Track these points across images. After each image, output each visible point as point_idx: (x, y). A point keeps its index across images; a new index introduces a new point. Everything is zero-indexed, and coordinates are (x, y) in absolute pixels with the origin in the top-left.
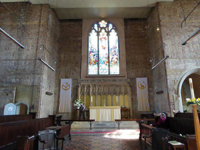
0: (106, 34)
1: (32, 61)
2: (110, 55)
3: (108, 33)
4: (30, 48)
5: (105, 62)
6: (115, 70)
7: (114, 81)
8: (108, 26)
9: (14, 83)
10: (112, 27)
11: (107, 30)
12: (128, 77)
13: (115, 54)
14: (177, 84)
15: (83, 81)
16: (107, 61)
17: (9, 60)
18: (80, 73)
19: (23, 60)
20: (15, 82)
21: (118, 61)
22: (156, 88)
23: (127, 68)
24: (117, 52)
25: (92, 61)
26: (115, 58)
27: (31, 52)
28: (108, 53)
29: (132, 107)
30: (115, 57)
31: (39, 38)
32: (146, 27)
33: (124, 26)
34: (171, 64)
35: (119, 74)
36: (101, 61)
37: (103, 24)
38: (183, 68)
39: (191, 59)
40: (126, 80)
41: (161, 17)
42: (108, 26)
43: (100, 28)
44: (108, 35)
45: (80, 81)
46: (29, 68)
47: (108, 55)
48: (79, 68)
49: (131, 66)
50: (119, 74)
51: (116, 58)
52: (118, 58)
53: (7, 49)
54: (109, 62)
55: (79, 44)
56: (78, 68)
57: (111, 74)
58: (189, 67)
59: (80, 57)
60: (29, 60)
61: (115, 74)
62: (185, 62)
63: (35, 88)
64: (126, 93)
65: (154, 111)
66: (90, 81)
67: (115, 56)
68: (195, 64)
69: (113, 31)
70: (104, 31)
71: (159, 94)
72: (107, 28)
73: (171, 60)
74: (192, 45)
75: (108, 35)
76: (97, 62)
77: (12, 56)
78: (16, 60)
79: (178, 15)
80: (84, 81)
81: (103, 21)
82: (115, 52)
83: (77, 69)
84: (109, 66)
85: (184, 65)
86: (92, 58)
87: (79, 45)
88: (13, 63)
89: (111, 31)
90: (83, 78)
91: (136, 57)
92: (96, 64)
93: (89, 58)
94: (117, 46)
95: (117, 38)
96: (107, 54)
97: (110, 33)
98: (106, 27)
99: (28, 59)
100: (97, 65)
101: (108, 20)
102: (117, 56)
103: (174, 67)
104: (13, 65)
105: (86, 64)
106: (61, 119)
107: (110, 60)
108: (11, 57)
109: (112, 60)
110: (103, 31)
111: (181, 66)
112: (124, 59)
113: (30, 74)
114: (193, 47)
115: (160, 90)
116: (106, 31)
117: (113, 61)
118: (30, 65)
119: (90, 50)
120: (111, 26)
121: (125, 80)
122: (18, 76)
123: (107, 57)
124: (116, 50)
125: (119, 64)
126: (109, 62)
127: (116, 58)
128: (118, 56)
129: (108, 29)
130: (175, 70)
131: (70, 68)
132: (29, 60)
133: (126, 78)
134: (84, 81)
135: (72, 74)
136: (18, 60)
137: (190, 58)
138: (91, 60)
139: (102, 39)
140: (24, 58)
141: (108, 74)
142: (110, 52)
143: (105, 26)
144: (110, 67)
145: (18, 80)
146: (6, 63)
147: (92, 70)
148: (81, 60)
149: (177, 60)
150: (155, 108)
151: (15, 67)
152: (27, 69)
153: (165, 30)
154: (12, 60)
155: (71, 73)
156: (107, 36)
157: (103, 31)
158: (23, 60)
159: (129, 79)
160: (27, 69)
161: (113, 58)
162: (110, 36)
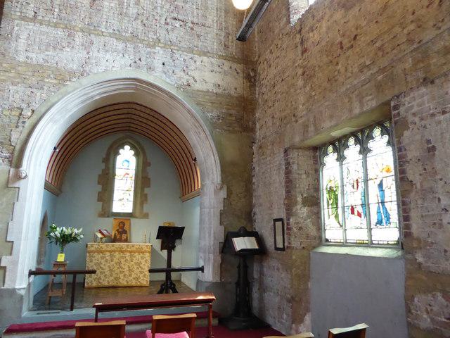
14: (28, 124)
34: (22, 41)
58: (101, 69)
62: (88, 46)
68: (128, 60)
103: (36, 57)
130: (38, 69)
137: (118, 35)
149: (60, 33)
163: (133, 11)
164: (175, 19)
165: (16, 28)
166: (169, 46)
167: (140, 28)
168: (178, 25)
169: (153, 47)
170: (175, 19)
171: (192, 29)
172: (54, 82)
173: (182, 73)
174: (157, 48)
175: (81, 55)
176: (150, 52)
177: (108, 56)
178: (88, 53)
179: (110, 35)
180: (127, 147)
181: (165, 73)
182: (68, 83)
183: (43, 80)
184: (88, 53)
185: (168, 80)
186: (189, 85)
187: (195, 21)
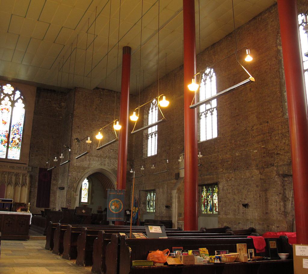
0: (10, 103)
2: (11, 133)
3: (13, 103)
5: (3, 142)
8: (14, 93)
10: (19, 96)
11: (12, 99)
13: (18, 133)
16: (6, 140)
21: (20, 143)
22: (60, 182)
23: (30, 153)
24: (21, 130)
26: (17, 138)
28: (8, 131)
30: (18, 136)
32: (63, 104)
33: (36, 97)
35: (18, 159)
37: (8, 89)
39: (97, 157)
41: (75, 105)
42: (14, 93)
43: (4, 94)
44: (13, 106)
47: (8, 132)
50: (18, 159)
51: (18, 139)
52: (21, 139)
54: (8, 142)
57: (8, 158)
58: (93, 166)
61: (13, 158)
62: (89, 160)
64: (23, 185)
65: (54, 209)
68: (99, 163)
69: (20, 101)
70: (9, 99)
71: (61, 190)
72: (13, 96)
75: (13, 106)
79: (94, 107)
81: (9, 85)
82: (17, 130)
84: (8, 147)
85: (88, 163)
89: (17, 101)
94: (22, 123)
95: (23, 111)
96: (7, 131)
97: (16, 104)
98: (11, 95)
101: (17, 84)
103: (78, 164)
107: (10, 140)
109: (12, 140)
110: (7, 98)
115: (62, 185)
116: (10, 100)
117: (13, 141)
120: (18, 93)
121: (25, 169)
123: (7, 135)
124: (20, 128)
125: (20, 147)
126: (8, 142)
127: (18, 139)
128: (21, 137)
129: (14, 97)
130: (79, 167)
133: (27, 166)
137: (97, 156)
139: (4, 110)
141: (4, 157)
142: (12, 129)
143: (10, 93)
144: (9, 149)
150: (55, 205)
153: (77, 122)
156: (11, 107)
157: (7, 98)
161: (14, 138)
162: (14, 108)
164: (111, 149)
165: (74, 157)
166: (109, 158)
169: (105, 158)
170: (111, 149)
171: (116, 152)
174: (106, 159)
175: (88, 163)
176: (104, 160)
177: (94, 162)
186: (114, 169)
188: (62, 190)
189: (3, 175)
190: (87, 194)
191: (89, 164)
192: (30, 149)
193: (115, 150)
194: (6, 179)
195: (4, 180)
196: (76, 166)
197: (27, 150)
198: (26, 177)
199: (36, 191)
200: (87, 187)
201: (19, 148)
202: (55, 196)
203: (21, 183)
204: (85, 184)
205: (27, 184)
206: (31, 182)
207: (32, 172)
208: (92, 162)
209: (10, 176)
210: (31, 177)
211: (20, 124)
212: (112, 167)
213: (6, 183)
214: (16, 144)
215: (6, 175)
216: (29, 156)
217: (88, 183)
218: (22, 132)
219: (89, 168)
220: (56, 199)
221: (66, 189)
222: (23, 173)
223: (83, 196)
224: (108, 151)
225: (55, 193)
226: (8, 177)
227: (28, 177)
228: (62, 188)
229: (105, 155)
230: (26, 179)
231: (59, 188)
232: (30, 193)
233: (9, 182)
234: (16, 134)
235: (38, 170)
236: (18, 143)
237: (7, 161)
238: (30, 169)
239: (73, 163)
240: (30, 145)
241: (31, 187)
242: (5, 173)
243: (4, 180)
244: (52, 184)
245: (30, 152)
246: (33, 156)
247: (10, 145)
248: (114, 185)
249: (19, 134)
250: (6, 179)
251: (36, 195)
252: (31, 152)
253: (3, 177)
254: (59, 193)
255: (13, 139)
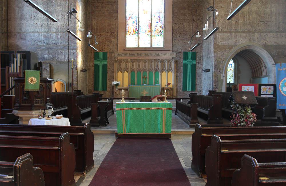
1: (64, 34)
4: (60, 17)
6: (159, 42)
7: (157, 55)
9: (46, 59)
12: (174, 50)
13: (160, 21)
15: (120, 54)
16: (150, 30)
17: (38, 32)
18: (117, 45)
19: (54, 33)
20: (48, 58)
21: (163, 31)
22: (204, 64)
23: (173, 39)
24: (162, 18)
25: (131, 30)
26: (158, 25)
27: (62, 23)
28: (150, 20)
29: (176, 86)
30: (160, 24)
31: (69, 5)
34: (220, 39)
35: (163, 46)
36: (141, 30)
38: (233, 44)
39: (244, 33)
40: (171, 54)
45: (117, 55)
46: (62, 42)
47: (150, 22)
48: (116, 38)
49: (178, 37)
50: (163, 46)
51: (160, 27)
52: (163, 26)
53: (33, 18)
54: (151, 31)
55: (114, 6)
56: (115, 39)
59: (117, 25)
60: (60, 32)
61: (158, 46)
62: (236, 37)
63: (71, 64)
64: (169, 70)
65: (200, 91)
66: (128, 55)
67: (159, 23)
71: (206, 72)
73: (221, 34)
74: (249, 15)
76: (137, 31)
77: (40, 28)
78: (44, 32)
80: (122, 55)
82: (159, 18)
83: (113, 40)
84: (151, 36)
85: (235, 40)
86: (130, 25)
87: (115, 9)
88: (43, 36)
90: (120, 51)
91: (185, 25)
92: (136, 34)
93: (127, 26)
96: (149, 21)
99: (60, 31)
100: (137, 34)
102: (161, 24)
103: (223, 43)
104: (43, 38)
105: (124, 33)
106: (102, 97)
108: (39, 29)
109: (155, 29)
111: (231, 42)
112: (170, 28)
113: (63, 49)
114: (249, 19)
115: (207, 68)
117: (156, 30)
118: (62, 38)
119: (128, 15)
122: (51, 51)
123: (149, 24)
125: (163, 34)
126: (151, 31)
127: (160, 27)
128: (163, 24)
131: (104, 39)
132: (60, 32)
134: (122, 55)
135: (108, 46)
136: (47, 32)
137: (244, 32)
138: (130, 28)
140: (54, 30)
141: (149, 46)
142: (153, 18)
144: (153, 38)
145: (51, 55)
146: (34, 36)
147: (131, 42)
148: (118, 29)
149: (228, 34)
150: (201, 88)
151: (46, 41)
152: (59, 44)
154: (41, 32)
155: (106, 45)
158: (54, 33)
159: (175, 53)
160: (59, 44)
161: (156, 26)
163: (248, 22)
164: (261, 21)
166: (259, 31)
167: (250, 27)
168: (262, 24)
169: (255, 33)
170: (261, 21)
171: (267, 24)
172: (228, 49)
173: (263, 40)
174: (256, 33)
176: (253, 35)
178: (236, 39)
179: (242, 32)
180: (242, 86)
181: (258, 41)
182: (232, 49)
183: (226, 49)
184: (236, 39)
185: (260, 44)
186: (266, 44)
187: (268, 20)
188: (207, 73)
189: (150, 63)
190: (233, 75)
191: (235, 42)
192: (173, 35)
193: (266, 22)
194: (153, 66)
195: (152, 67)
196: (221, 45)
197: (170, 37)
198: (171, 63)
199: (182, 75)
200: (233, 68)
201: (162, 36)
202: (200, 79)
203: (167, 69)
204: (231, 66)
205: (173, 69)
206: (176, 67)
207: (177, 58)
208: (239, 39)
209: (156, 63)
210: (176, 62)
211: (160, 11)
212: (263, 42)
213: (153, 70)
214: (159, 32)
215: (152, 63)
216: (172, 42)
217: (233, 64)
218: (163, 20)
219: (235, 46)
220: (202, 82)
221: (211, 71)
222: (168, 59)
223: (229, 77)
224: (257, 24)
225: (200, 76)
226: (154, 64)
227: (173, 63)
228: (208, 71)
229: (254, 29)
230: (171, 65)
231: (204, 71)
232: (176, 77)
233: (156, 69)
234: (158, 22)
235: (182, 54)
236: (161, 31)
237: (152, 49)
238: (175, 55)
239: (217, 42)
240: (172, 31)
241: (176, 72)
242: (151, 61)
243: (152, 67)
244: (197, 67)
245: (173, 37)
246: (176, 42)
247: (153, 34)
248: (265, 62)
249: (161, 21)
250: (153, 66)
251: (182, 79)
252: (174, 38)
253: (150, 65)
254: (204, 75)
255: (156, 28)
